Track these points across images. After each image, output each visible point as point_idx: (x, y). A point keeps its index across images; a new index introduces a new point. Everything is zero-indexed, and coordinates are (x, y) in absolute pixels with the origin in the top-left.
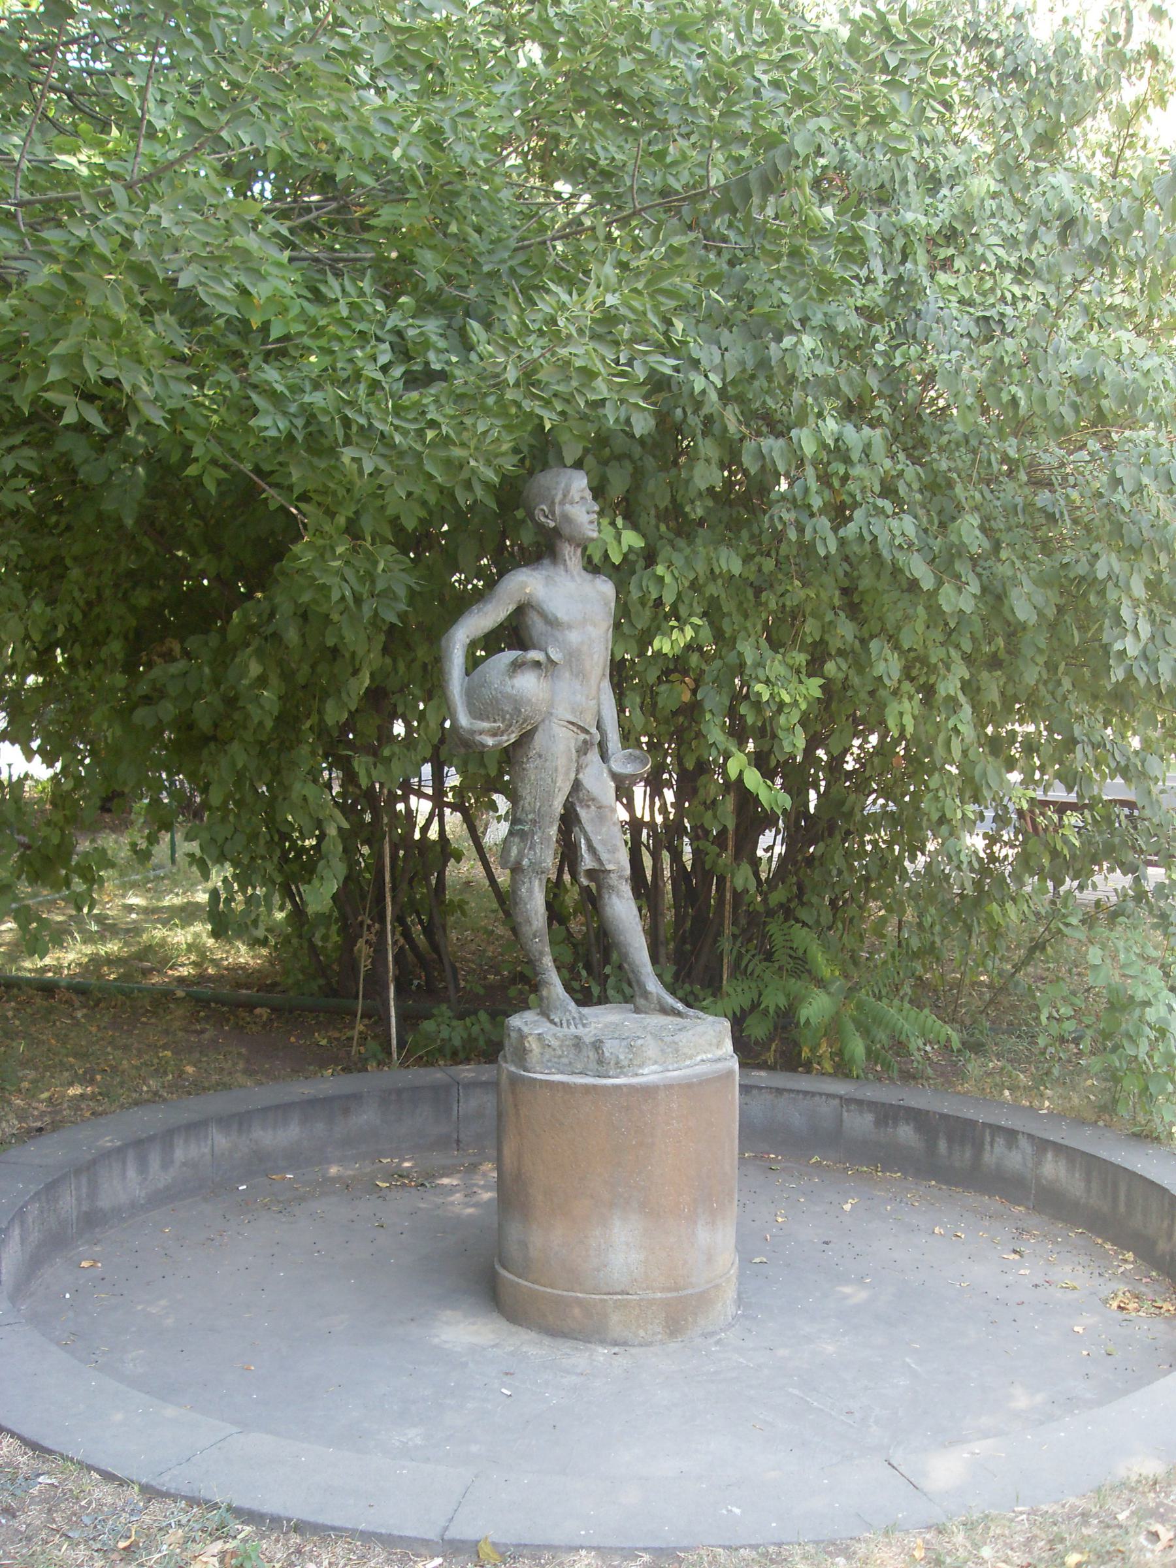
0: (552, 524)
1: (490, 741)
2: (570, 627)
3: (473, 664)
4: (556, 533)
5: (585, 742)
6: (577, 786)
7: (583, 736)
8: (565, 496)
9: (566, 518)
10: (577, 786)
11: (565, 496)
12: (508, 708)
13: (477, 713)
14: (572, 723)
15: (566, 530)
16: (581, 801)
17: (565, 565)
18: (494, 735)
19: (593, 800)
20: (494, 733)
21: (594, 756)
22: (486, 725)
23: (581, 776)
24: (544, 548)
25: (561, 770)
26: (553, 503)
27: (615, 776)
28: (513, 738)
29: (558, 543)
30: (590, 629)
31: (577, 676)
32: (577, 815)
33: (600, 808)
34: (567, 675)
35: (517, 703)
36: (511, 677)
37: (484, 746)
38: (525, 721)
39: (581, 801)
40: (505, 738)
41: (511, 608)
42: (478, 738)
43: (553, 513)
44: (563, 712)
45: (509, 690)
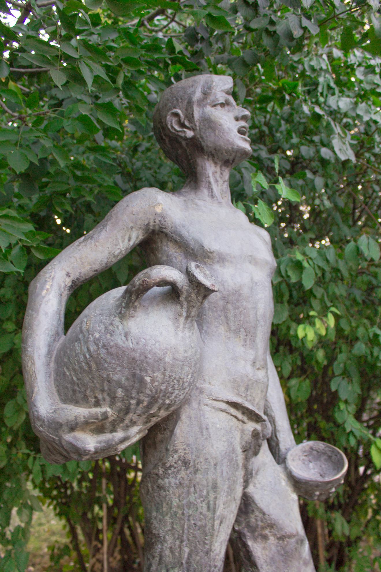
0: (190, 134)
1: (90, 442)
2: (222, 259)
3: (73, 310)
4: (196, 146)
5: (255, 435)
6: (247, 505)
7: (251, 426)
8: (206, 94)
9: (209, 123)
10: (247, 505)
11: (206, 94)
12: (119, 376)
13: (70, 390)
14: (235, 405)
15: (209, 140)
16: (253, 530)
17: (210, 188)
18: (100, 430)
19: (271, 526)
20: (99, 426)
21: (265, 454)
22: (81, 412)
23: (251, 489)
24: (181, 161)
25: (223, 486)
26: (190, 103)
27: (297, 483)
28: (136, 433)
29: (199, 161)
30: (251, 268)
31: (237, 332)
32: (249, 554)
33: (282, 538)
34: (222, 330)
35: (136, 366)
36: (122, 317)
37: (80, 452)
38: (153, 400)
39: (253, 530)
40: (119, 435)
41: (136, 236)
42: (68, 437)
43: (190, 117)
44: (218, 385)
45: (120, 340)
